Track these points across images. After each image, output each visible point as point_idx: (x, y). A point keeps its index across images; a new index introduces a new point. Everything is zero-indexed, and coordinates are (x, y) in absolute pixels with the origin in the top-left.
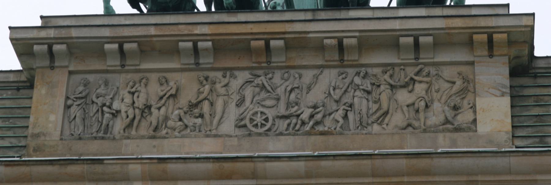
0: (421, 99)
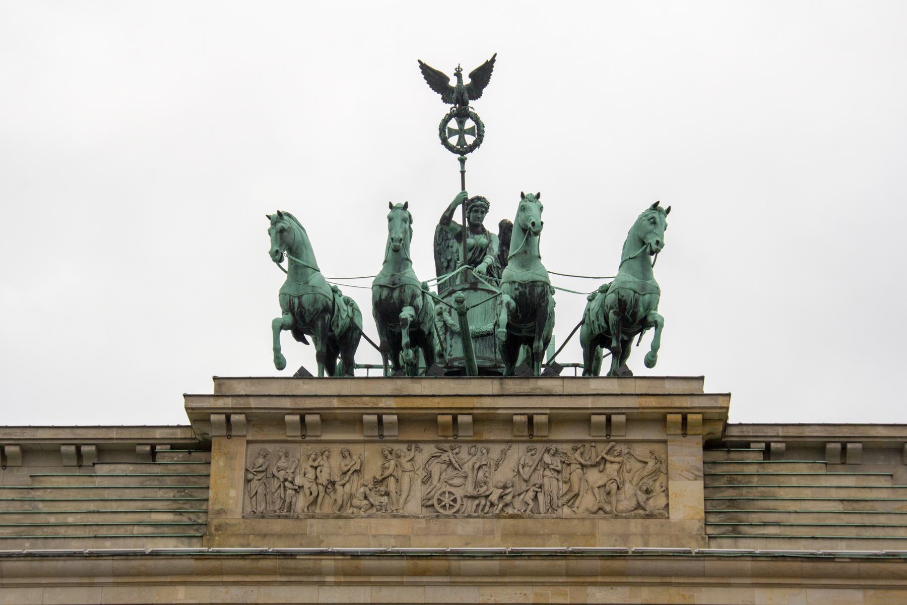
0: (613, 481)
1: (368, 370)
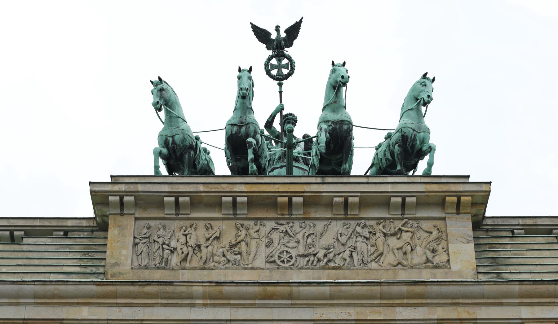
0: (408, 244)
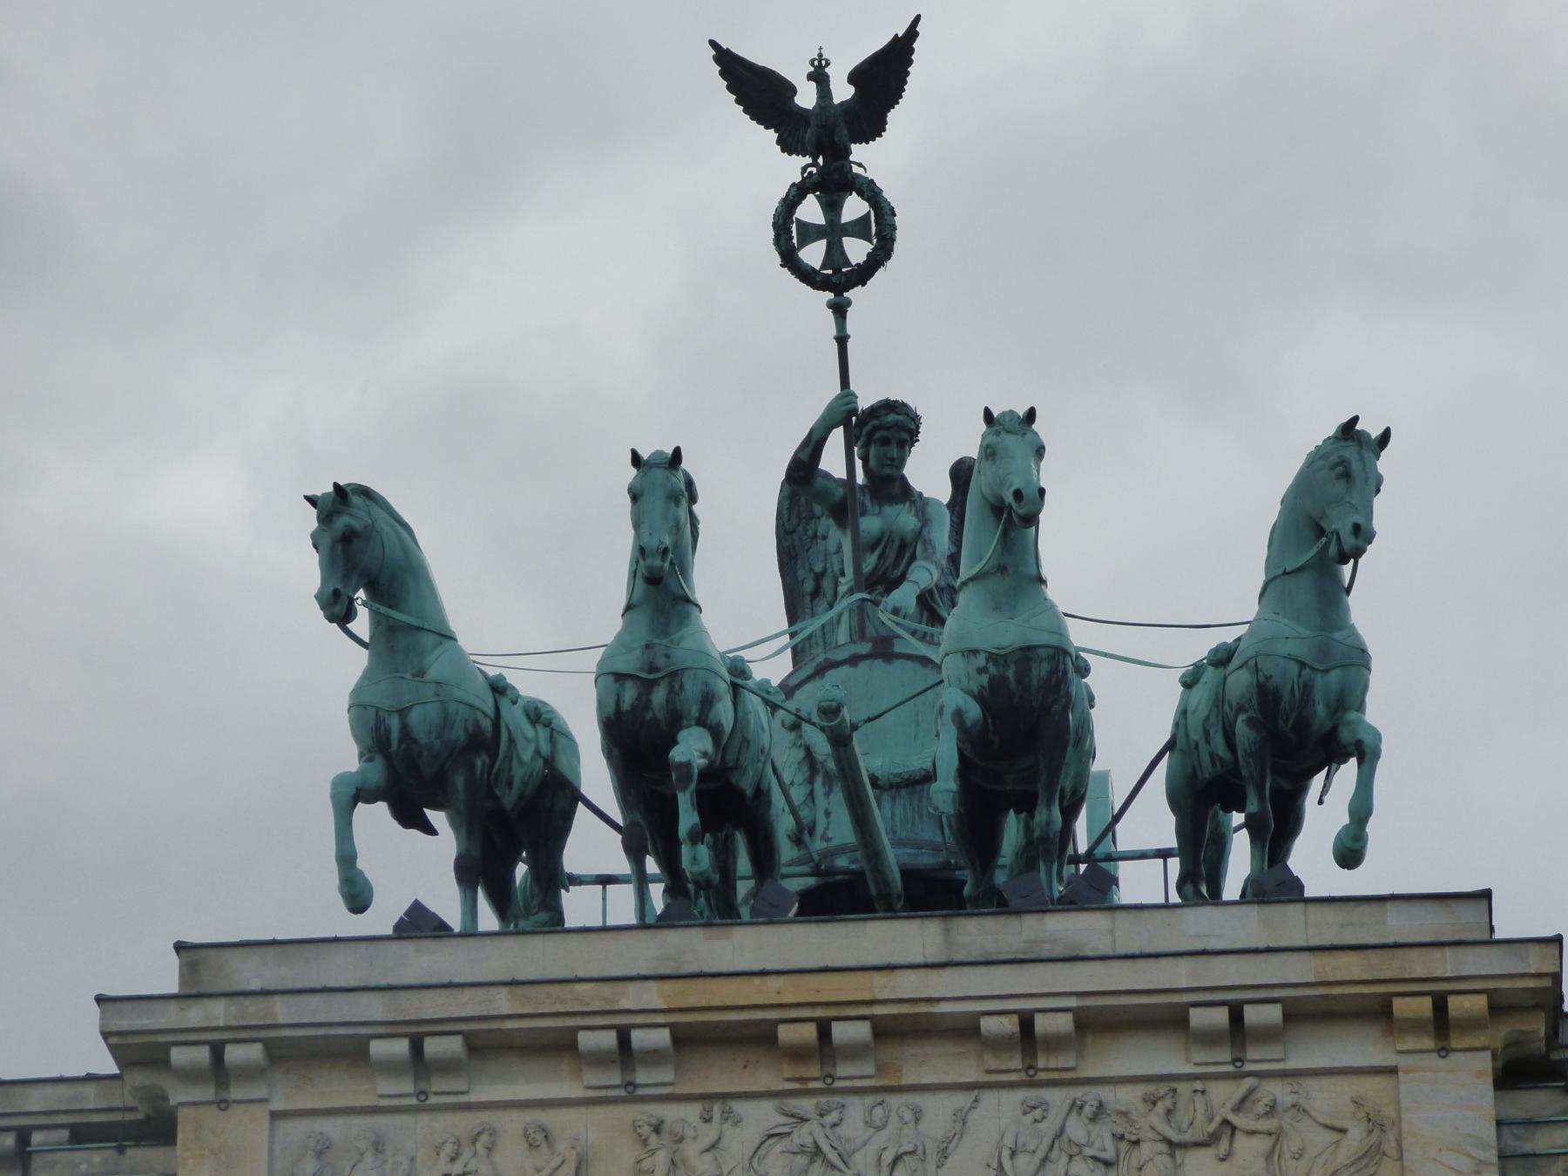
1: (604, 888)
